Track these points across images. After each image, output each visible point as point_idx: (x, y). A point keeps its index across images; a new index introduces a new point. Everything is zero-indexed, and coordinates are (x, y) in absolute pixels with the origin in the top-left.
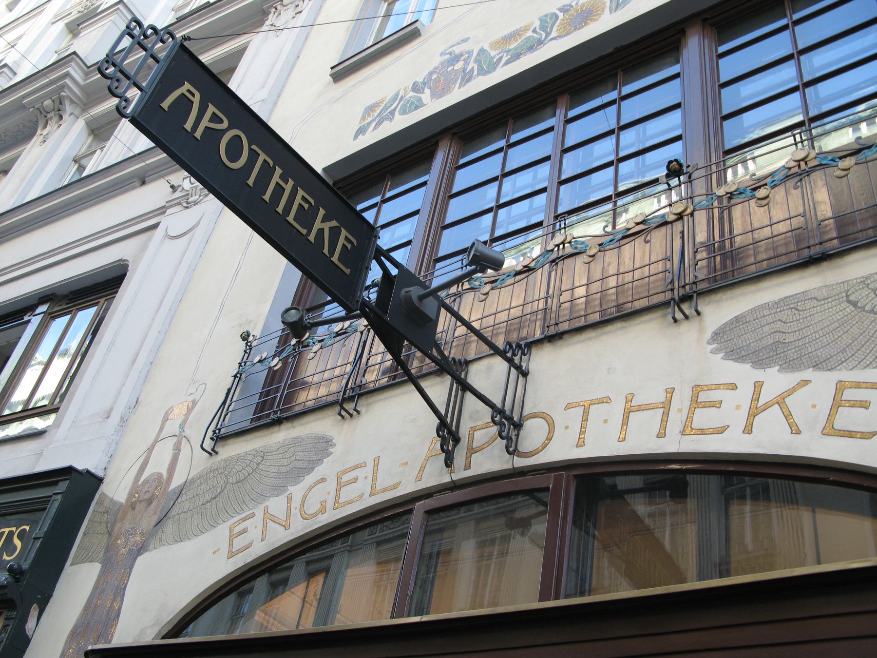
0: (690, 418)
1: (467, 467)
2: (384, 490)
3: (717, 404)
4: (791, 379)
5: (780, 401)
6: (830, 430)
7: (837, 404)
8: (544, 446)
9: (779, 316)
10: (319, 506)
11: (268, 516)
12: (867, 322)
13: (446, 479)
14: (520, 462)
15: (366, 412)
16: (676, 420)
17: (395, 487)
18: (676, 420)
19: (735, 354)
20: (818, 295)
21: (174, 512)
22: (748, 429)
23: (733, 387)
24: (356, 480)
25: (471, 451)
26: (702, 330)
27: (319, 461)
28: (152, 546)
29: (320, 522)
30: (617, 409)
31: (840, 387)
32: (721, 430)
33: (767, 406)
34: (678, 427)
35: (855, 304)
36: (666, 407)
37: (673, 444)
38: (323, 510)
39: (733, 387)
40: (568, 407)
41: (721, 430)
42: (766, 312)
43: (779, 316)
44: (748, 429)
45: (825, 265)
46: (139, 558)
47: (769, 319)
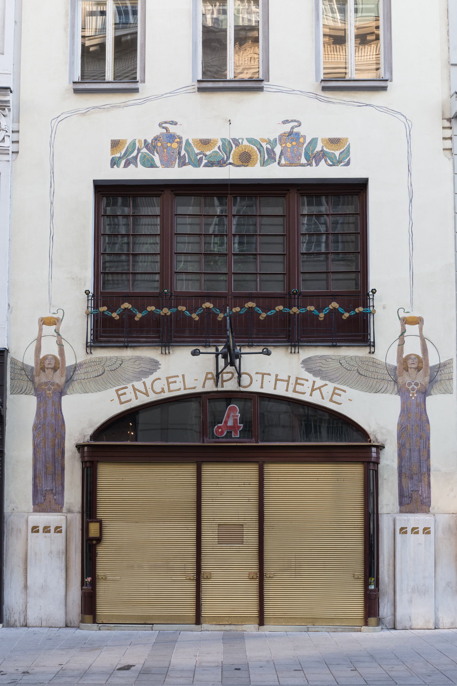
0: (295, 388)
1: (222, 386)
2: (190, 389)
3: (303, 385)
4: (324, 382)
5: (319, 388)
6: (331, 400)
7: (334, 393)
8: (250, 385)
9: (321, 361)
10: (161, 390)
11: (135, 389)
12: (343, 371)
13: (215, 389)
14: (242, 389)
15: (173, 353)
16: (291, 388)
17: (194, 388)
18: (291, 388)
19: (309, 370)
20: (332, 357)
21: (75, 377)
22: (311, 395)
23: (307, 381)
24: (175, 382)
25: (223, 381)
26: (299, 359)
27: (155, 370)
28: (68, 392)
29: (164, 396)
30: (273, 378)
31: (335, 388)
32: (304, 393)
33: (316, 389)
34: (292, 389)
35: (341, 364)
36: (288, 381)
37: (290, 394)
38: (163, 391)
39: (307, 381)
40: (257, 373)
41: (304, 393)
42: (318, 359)
43: (321, 361)
44: (311, 395)
45: (335, 348)
46: (63, 398)
47: (319, 361)
